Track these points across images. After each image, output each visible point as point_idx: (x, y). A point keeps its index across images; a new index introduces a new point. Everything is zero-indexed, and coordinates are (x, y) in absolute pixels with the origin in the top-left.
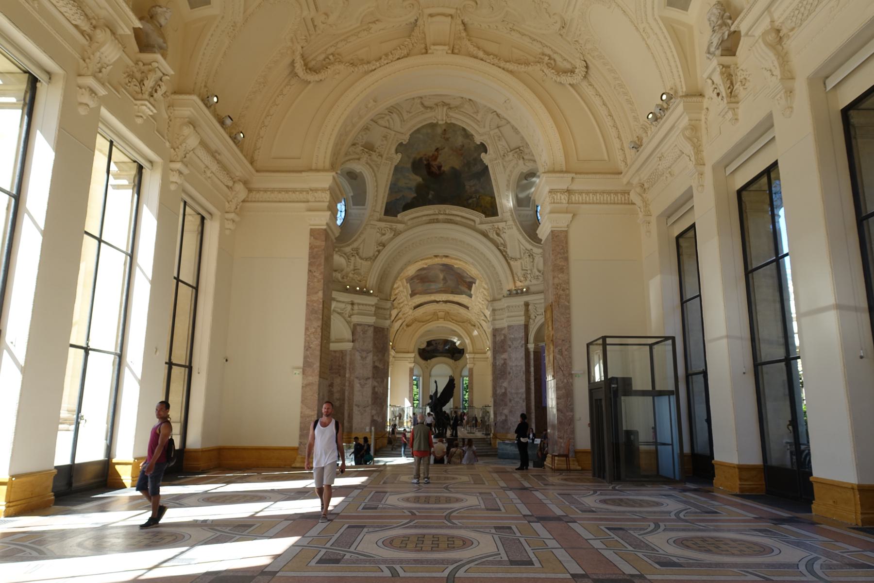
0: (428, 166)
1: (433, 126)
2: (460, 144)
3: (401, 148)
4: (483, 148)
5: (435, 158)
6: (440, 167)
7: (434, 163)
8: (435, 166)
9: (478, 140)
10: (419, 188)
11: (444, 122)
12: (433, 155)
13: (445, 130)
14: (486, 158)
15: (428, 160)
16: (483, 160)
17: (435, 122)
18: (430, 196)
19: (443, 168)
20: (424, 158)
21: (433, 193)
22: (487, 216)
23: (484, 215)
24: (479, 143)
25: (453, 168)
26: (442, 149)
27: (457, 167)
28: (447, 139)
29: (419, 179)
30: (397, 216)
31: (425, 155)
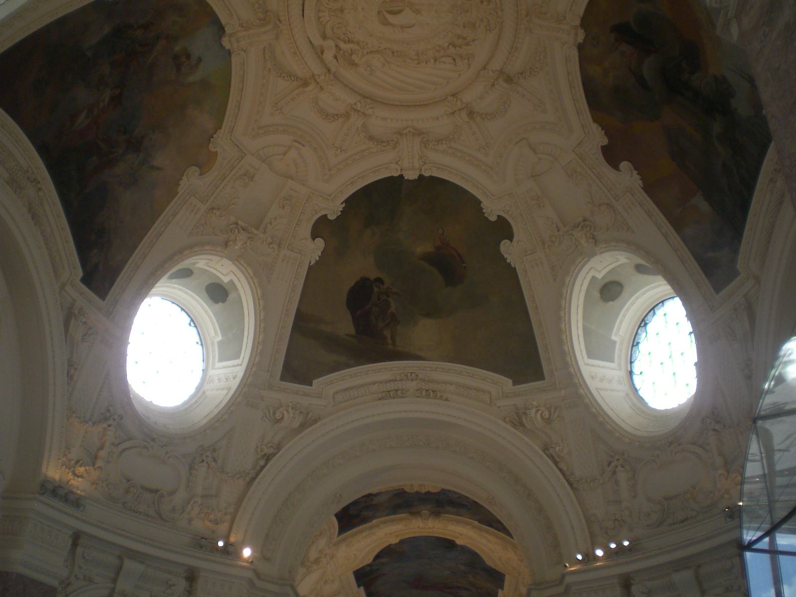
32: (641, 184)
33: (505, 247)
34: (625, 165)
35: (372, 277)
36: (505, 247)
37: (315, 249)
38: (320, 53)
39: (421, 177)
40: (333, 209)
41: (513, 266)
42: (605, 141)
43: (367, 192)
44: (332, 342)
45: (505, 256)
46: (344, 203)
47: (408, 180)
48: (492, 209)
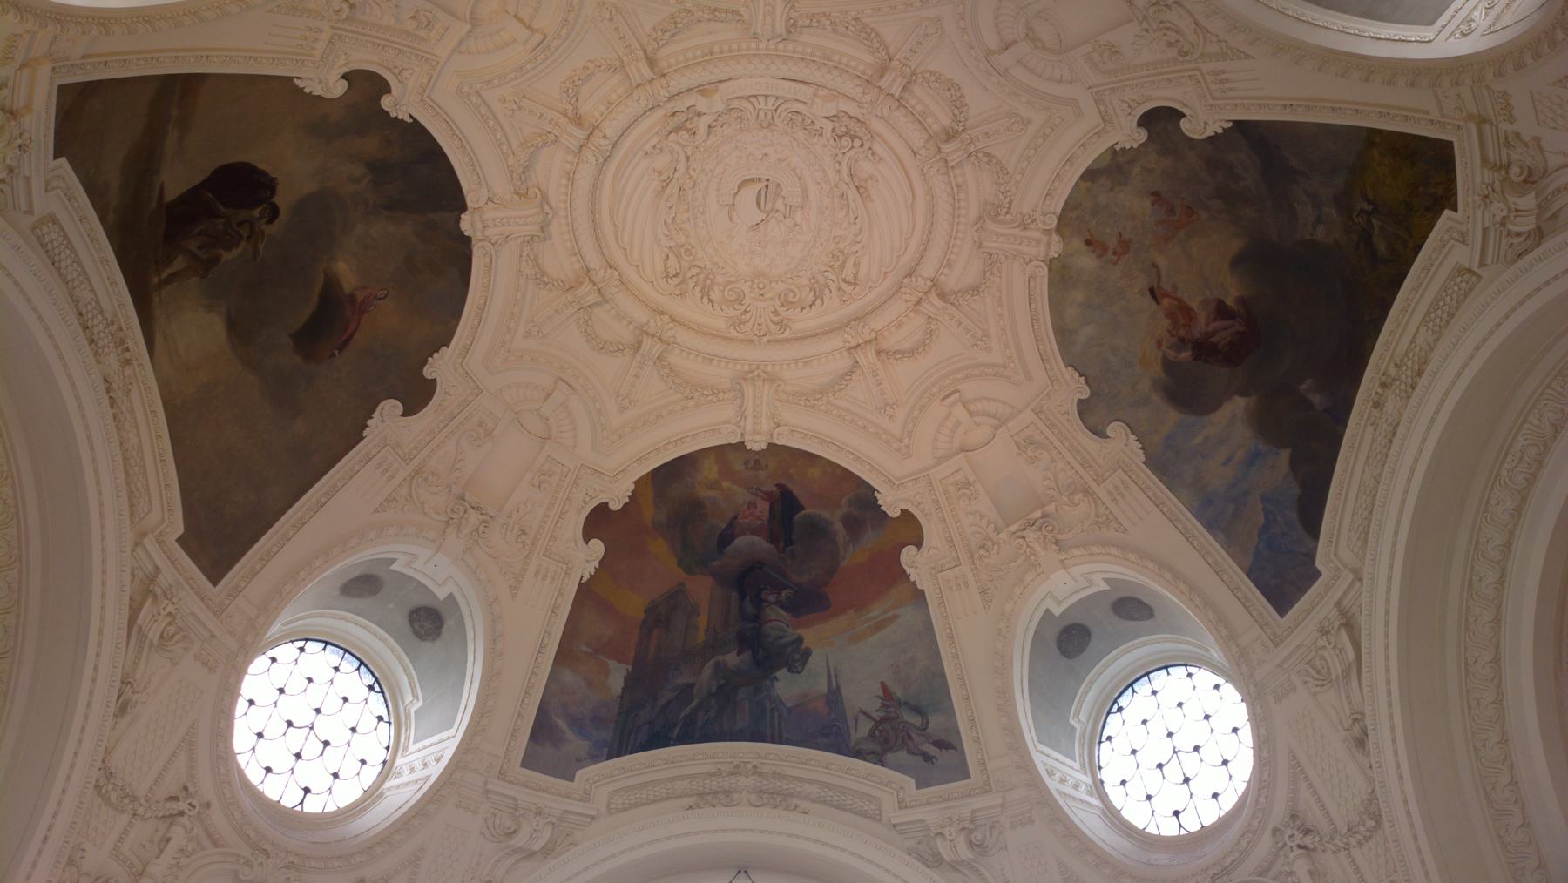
0: (1204, 349)
1: (1061, 276)
2: (1147, 203)
3: (1092, 415)
4: (1160, 121)
5: (1186, 310)
6: (1222, 311)
7: (1203, 323)
8: (1210, 328)
9: (1130, 135)
10: (1268, 424)
11: (1056, 238)
12: (1170, 315)
13: (1088, 243)
14: (1202, 123)
15: (1182, 340)
16: (1210, 133)
17: (1044, 271)
18: (1316, 399)
19: (1230, 302)
20: (1171, 354)
21: (1308, 383)
22: (1446, 198)
23: (1447, 213)
24: (1142, 136)
25: (1237, 262)
26: (1159, 278)
27: (1236, 245)
28: (1125, 246)
29: (1237, 406)
30: (1317, 574)
31: (1159, 344)
32: (584, 580)
33: (390, 408)
34: (597, 547)
35: (277, 200)
36: (390, 408)
37: (327, 83)
38: (702, 90)
39: (467, 241)
40: (400, 104)
41: (365, 433)
42: (615, 506)
43: (432, 155)
44: (144, 162)
45: (376, 415)
46: (411, 121)
47: (460, 218)
48: (440, 367)
